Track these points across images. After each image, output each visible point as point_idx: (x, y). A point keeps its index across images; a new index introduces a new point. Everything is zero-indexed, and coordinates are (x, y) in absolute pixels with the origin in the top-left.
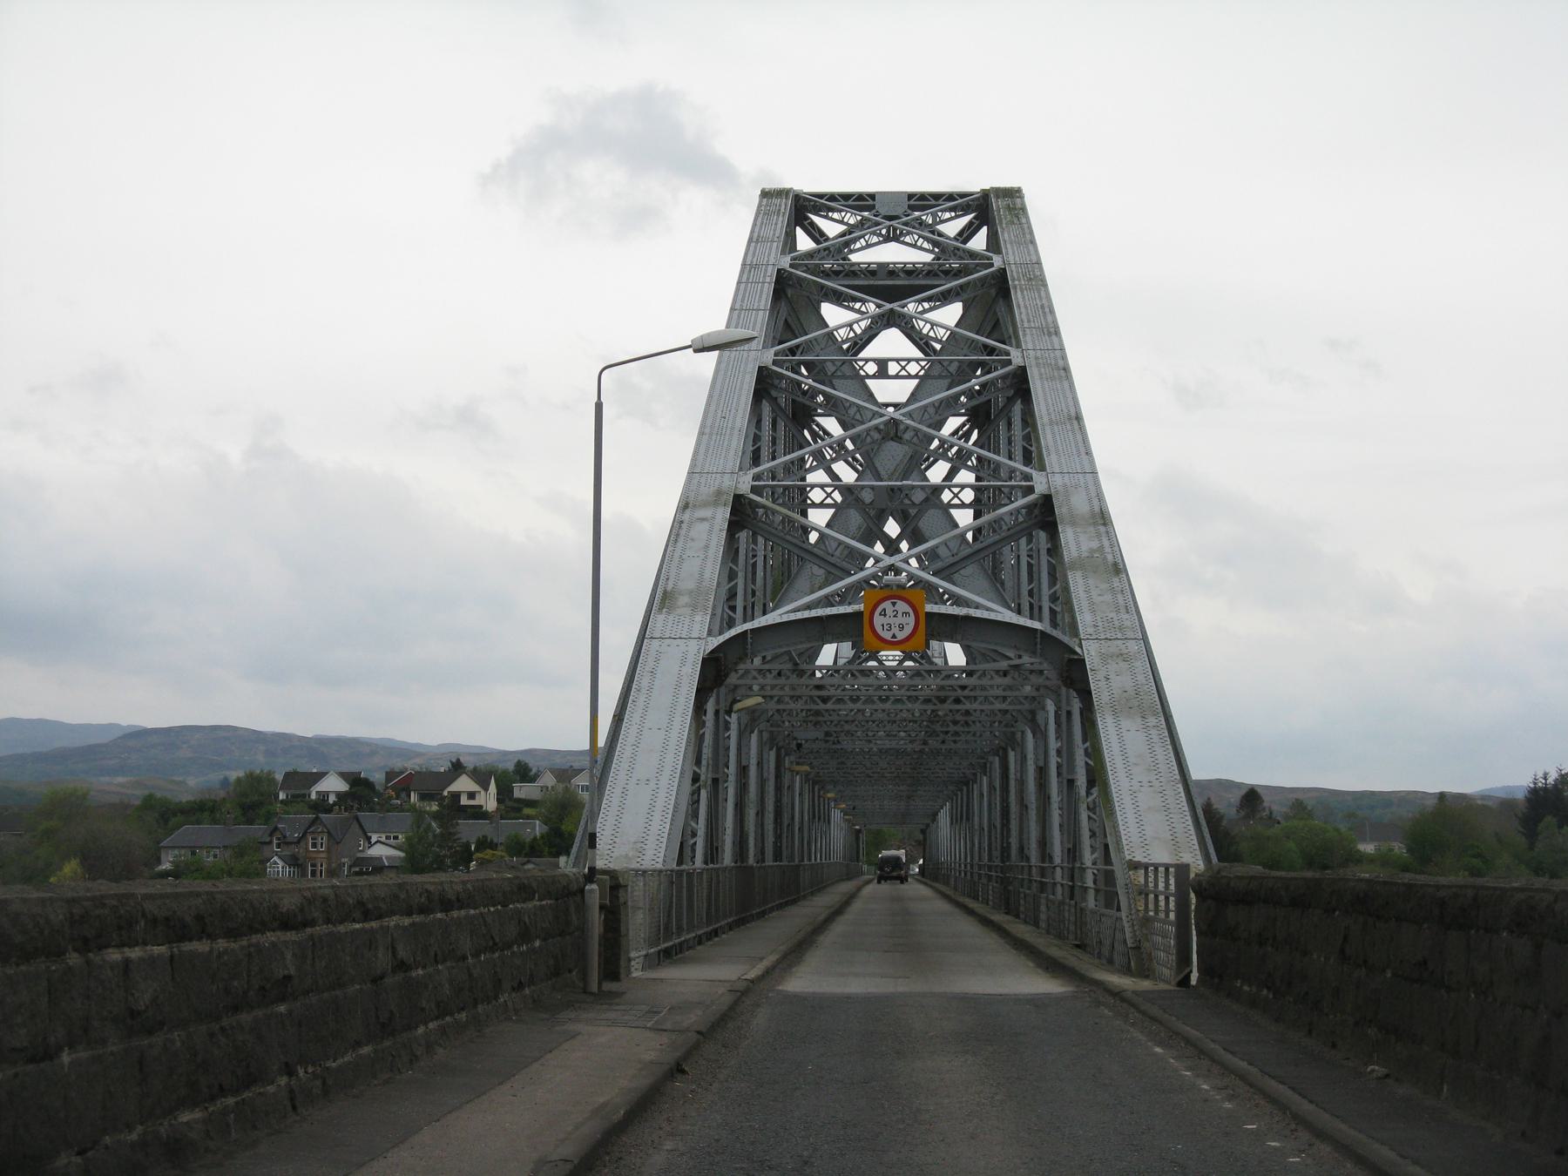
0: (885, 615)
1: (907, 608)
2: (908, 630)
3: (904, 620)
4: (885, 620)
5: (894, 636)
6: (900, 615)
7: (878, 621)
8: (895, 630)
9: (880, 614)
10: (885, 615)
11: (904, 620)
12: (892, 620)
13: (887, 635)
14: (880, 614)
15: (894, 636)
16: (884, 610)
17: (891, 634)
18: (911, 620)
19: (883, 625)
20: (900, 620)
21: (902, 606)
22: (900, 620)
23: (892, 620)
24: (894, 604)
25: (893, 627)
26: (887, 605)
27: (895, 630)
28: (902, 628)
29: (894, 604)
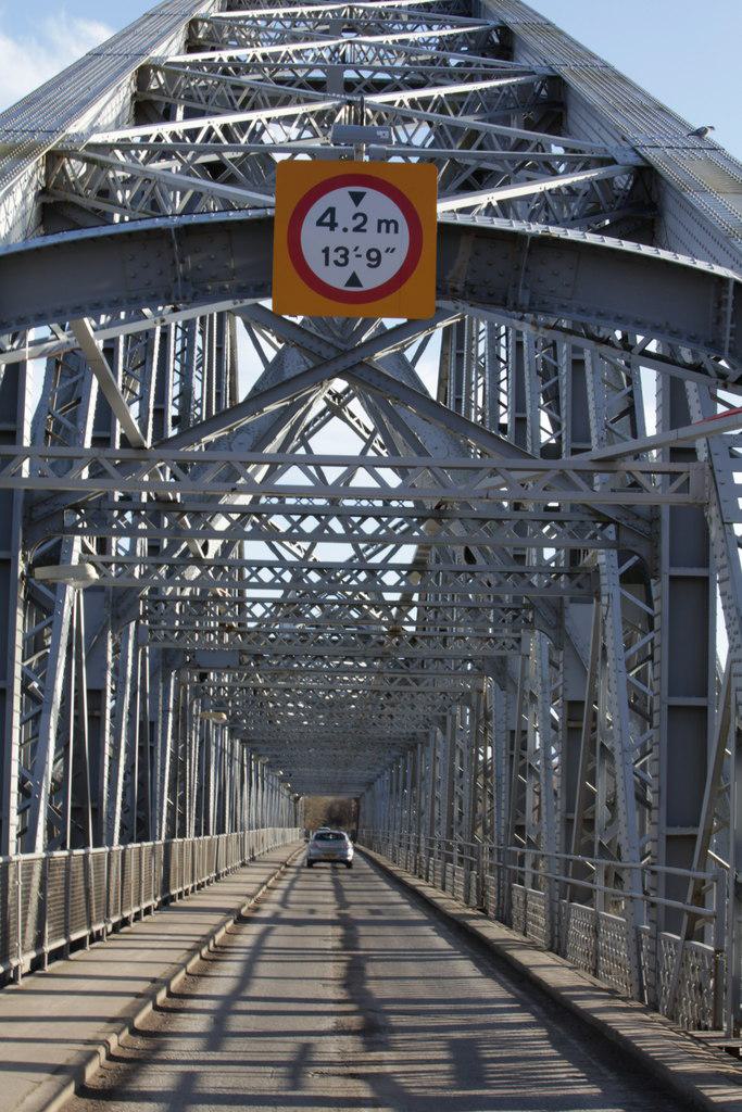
0: (333, 225)
1: (395, 212)
2: (391, 265)
3: (381, 241)
4: (335, 239)
5: (354, 281)
6: (371, 225)
7: (313, 239)
8: (358, 266)
9: (320, 223)
10: (333, 225)
11: (381, 241)
12: (351, 240)
13: (336, 278)
14: (320, 223)
15: (354, 281)
16: (331, 211)
17: (346, 274)
18: (401, 241)
19: (326, 251)
20: (372, 239)
21: (378, 205)
22: (372, 239)
23: (351, 240)
24: (357, 198)
25: (351, 256)
26: (339, 198)
27: (358, 266)
28: (375, 259)
29: (357, 198)
